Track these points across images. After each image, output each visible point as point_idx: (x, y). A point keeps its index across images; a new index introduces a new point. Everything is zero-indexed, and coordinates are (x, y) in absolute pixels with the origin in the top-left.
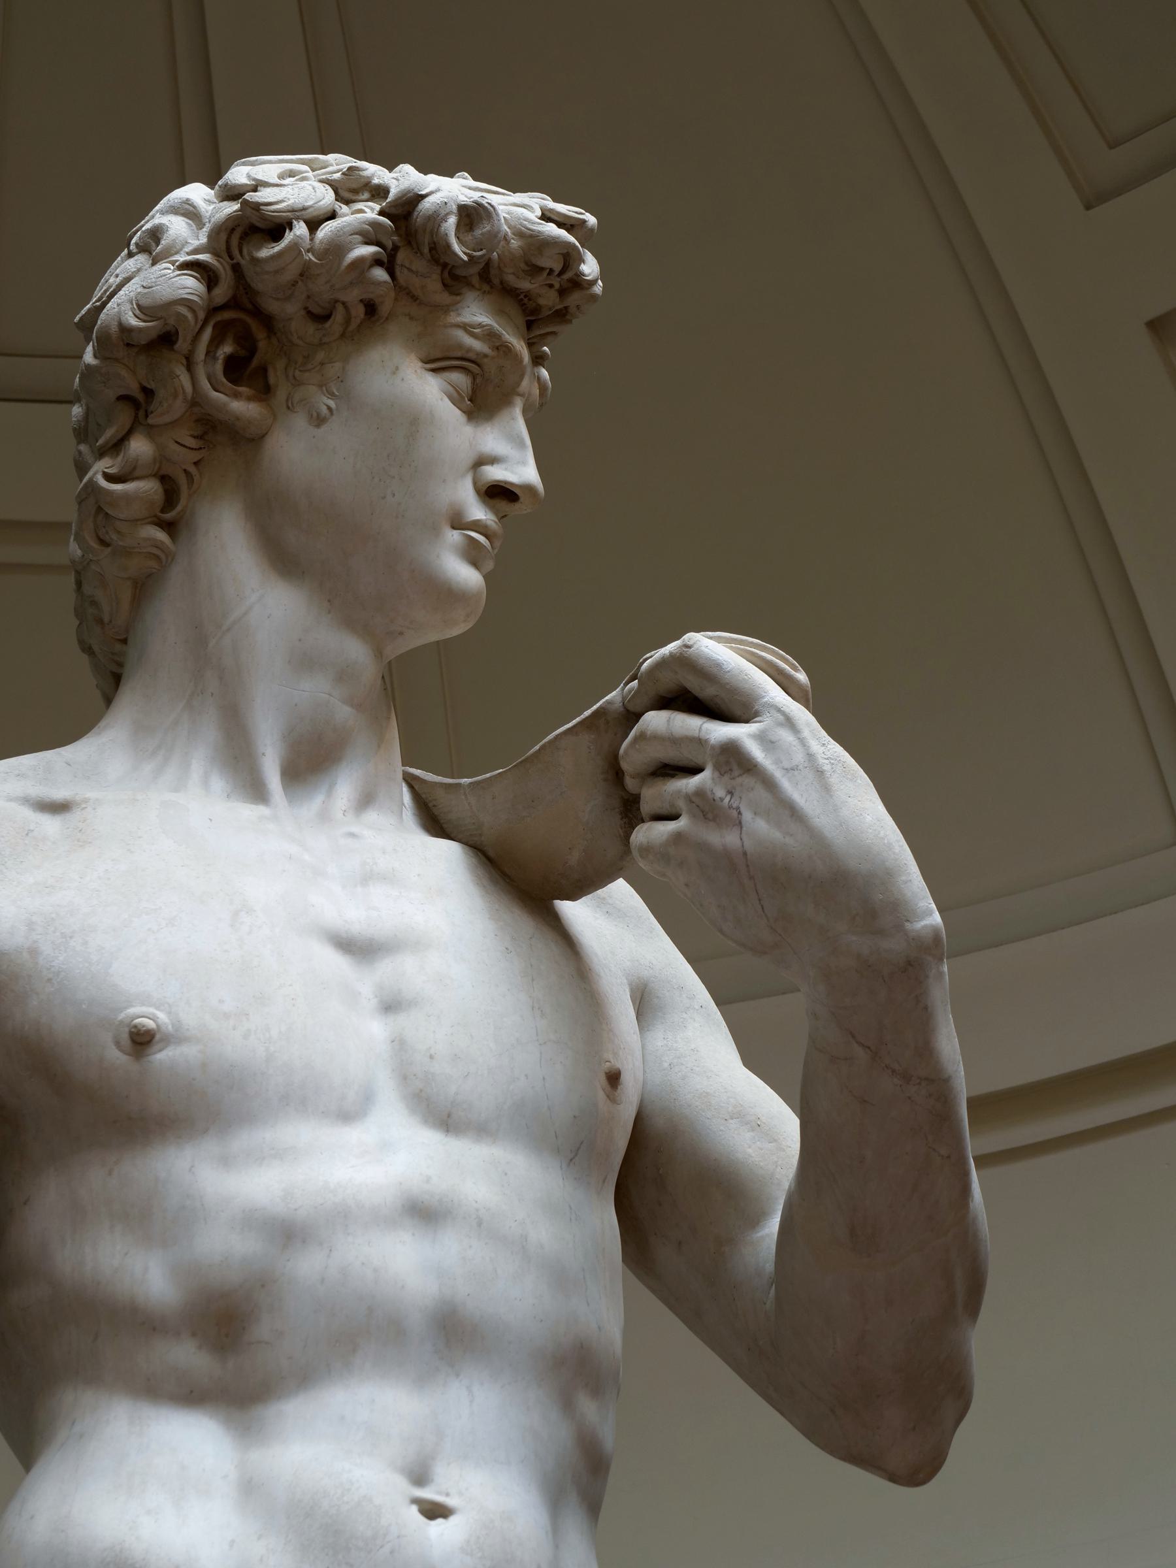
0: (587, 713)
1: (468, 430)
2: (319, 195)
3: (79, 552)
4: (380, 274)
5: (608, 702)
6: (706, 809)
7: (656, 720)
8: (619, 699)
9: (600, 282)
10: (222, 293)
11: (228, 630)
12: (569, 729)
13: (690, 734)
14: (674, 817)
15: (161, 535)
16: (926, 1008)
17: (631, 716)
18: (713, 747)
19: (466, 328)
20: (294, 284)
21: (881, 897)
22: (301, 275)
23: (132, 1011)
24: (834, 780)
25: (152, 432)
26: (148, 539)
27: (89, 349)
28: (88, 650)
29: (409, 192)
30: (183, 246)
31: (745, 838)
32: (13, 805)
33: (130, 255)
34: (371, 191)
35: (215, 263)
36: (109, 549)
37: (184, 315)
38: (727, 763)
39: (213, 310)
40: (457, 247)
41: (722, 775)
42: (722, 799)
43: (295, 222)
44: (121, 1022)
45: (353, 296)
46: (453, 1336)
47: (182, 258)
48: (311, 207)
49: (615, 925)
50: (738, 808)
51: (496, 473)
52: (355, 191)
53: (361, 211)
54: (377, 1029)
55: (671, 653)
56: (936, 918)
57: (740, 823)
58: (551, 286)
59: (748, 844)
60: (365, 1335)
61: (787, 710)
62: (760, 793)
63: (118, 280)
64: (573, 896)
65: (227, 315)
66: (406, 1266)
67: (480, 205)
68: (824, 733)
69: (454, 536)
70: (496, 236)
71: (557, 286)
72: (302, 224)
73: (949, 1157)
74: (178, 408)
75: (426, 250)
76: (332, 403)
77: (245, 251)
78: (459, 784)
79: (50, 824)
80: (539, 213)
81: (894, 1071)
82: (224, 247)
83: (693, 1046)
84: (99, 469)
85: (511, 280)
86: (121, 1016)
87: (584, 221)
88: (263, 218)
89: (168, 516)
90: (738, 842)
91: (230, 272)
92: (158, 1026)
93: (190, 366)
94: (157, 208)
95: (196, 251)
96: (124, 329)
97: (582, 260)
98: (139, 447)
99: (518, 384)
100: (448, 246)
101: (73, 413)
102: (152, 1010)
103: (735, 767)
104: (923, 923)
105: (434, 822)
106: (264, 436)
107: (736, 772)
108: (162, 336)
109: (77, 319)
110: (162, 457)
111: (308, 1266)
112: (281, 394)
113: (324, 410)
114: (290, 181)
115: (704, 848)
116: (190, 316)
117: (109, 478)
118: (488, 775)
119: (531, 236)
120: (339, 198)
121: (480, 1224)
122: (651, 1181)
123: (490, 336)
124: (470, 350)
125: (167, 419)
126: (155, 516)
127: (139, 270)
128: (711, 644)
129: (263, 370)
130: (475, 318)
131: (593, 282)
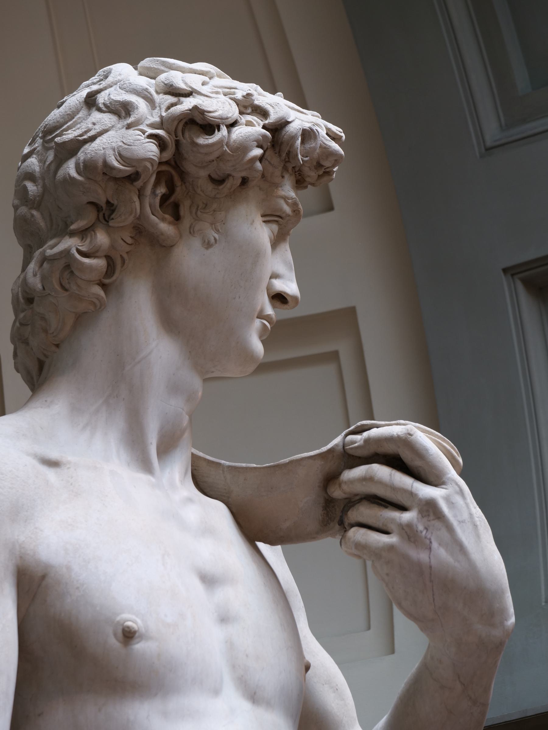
0: (324, 449)
3: (39, 286)
4: (258, 165)
5: (336, 445)
6: (409, 533)
7: (381, 471)
8: (341, 444)
11: (139, 362)
15: (102, 293)
18: (420, 500)
19: (285, 198)
21: (498, 605)
22: (218, 158)
23: (125, 616)
25: (109, 230)
26: (94, 294)
29: (283, 119)
34: (252, 108)
35: (168, 138)
36: (68, 293)
37: (148, 168)
38: (428, 511)
39: (160, 163)
40: (300, 157)
41: (423, 517)
43: (222, 126)
44: (118, 622)
47: (150, 131)
48: (230, 117)
50: (430, 539)
51: (280, 285)
52: (246, 107)
55: (399, 436)
57: (430, 548)
63: (98, 128)
65: (164, 168)
67: (312, 130)
69: (257, 323)
75: (284, 155)
76: (217, 236)
77: (187, 135)
78: (219, 464)
79: (51, 474)
84: (70, 243)
86: (118, 618)
89: (107, 281)
93: (140, 196)
95: (152, 126)
96: (106, 164)
98: (102, 238)
100: (297, 155)
102: (133, 617)
103: (431, 514)
106: (172, 246)
107: (432, 517)
110: (112, 246)
112: (187, 221)
113: (212, 240)
115: (406, 557)
116: (150, 167)
117: (78, 251)
119: (325, 148)
124: (284, 212)
125: (121, 225)
126: (100, 280)
127: (113, 126)
130: (290, 193)
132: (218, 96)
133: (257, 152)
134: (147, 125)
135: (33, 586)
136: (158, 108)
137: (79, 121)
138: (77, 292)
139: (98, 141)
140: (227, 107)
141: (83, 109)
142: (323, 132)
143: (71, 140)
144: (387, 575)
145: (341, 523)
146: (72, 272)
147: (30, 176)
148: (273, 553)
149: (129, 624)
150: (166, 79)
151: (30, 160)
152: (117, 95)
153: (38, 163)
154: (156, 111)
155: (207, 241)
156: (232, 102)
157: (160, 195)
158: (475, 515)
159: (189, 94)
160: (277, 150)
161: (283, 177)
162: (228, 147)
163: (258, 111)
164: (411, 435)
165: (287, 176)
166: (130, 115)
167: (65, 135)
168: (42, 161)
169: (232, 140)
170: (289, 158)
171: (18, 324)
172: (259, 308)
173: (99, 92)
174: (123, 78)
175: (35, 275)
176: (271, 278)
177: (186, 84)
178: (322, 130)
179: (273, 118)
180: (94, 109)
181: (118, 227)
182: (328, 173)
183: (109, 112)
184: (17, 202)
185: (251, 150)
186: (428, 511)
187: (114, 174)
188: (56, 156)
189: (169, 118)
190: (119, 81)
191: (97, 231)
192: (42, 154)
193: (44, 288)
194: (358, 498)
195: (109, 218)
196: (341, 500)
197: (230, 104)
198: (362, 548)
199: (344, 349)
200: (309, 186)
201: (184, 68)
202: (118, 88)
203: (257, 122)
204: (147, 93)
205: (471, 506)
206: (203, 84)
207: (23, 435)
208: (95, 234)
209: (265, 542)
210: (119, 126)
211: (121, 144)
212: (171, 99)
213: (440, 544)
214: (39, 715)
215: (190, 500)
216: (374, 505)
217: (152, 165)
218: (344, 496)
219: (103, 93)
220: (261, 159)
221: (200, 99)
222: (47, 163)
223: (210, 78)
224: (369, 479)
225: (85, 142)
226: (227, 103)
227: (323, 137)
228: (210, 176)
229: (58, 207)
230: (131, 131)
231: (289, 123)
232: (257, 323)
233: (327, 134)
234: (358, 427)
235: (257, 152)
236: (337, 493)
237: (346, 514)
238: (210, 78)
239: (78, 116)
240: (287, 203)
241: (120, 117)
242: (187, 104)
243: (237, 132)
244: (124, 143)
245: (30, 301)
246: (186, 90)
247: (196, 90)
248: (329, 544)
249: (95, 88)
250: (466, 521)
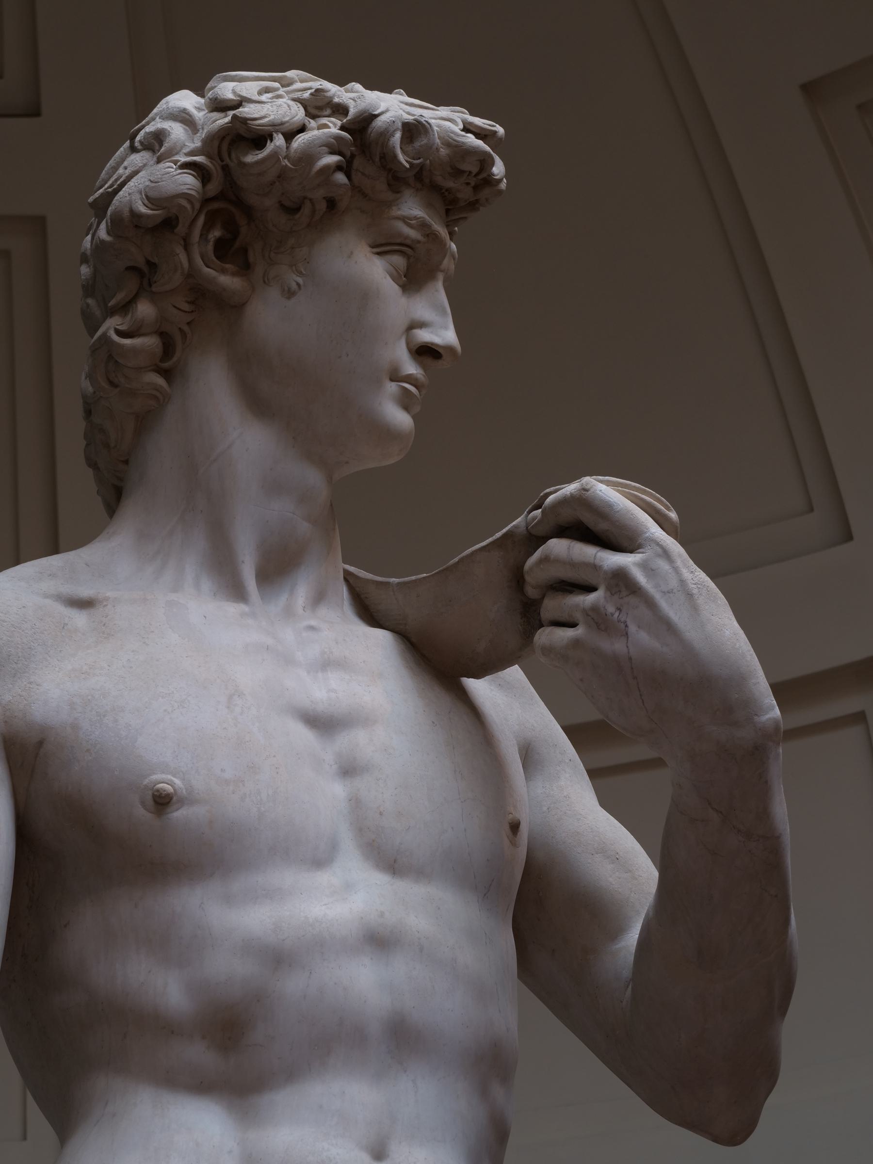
0: (498, 535)
1: (403, 301)
2: (293, 111)
3: (90, 389)
4: (341, 177)
5: (515, 527)
6: (598, 620)
7: (558, 546)
8: (523, 524)
9: (505, 180)
10: (213, 188)
14: (573, 625)
15: (160, 381)
16: (766, 782)
17: (534, 539)
18: (606, 572)
19: (405, 220)
20: (273, 183)
22: (279, 177)
23: (154, 777)
24: (700, 601)
27: (103, 226)
28: (92, 464)
30: (182, 148)
32: (48, 602)
33: (133, 149)
34: (332, 108)
35: (209, 164)
39: (206, 201)
40: (401, 157)
42: (612, 615)
43: (275, 135)
45: (319, 194)
46: (402, 1040)
47: (183, 159)
48: (287, 122)
49: (508, 699)
51: (425, 336)
52: (320, 108)
53: (326, 126)
54: (338, 790)
55: (571, 494)
56: (777, 712)
58: (468, 184)
60: (337, 1040)
61: (664, 544)
63: (128, 172)
64: (477, 676)
65: (216, 205)
66: (365, 984)
68: (691, 562)
69: (392, 388)
70: (431, 148)
71: (473, 184)
72: (281, 136)
73: (776, 896)
75: (377, 159)
76: (300, 280)
77: (233, 155)
78: (388, 583)
79: (79, 619)
80: (461, 126)
82: (216, 152)
83: (565, 794)
84: (110, 326)
85: (439, 180)
87: (495, 132)
88: (249, 130)
89: (166, 365)
92: (175, 790)
93: (187, 247)
94: (155, 111)
95: (192, 153)
96: (135, 215)
97: (493, 163)
98: (145, 309)
99: (441, 263)
100: (395, 156)
101: (82, 272)
102: (170, 777)
105: (369, 613)
108: (165, 221)
109: (91, 199)
111: (293, 985)
114: (270, 97)
116: (188, 206)
117: (119, 333)
118: (413, 578)
119: (456, 146)
120: (308, 114)
121: (421, 950)
122: (539, 906)
123: (423, 226)
124: (407, 237)
127: (145, 165)
128: (602, 487)
129: (245, 251)
130: (412, 212)
131: (501, 180)
133: (333, 159)
143: (102, 194)
144: (581, 680)
156: (291, 103)
162: (289, 161)
169: (292, 151)
185: (320, 158)
197: (289, 106)
204: (184, 115)
211: (148, 183)
212: (215, 115)
214: (65, 926)
226: (285, 106)
227: (453, 132)
228: (283, 207)
230: (161, 165)
235: (333, 159)
236: (531, 592)
247: (245, 98)
250: (675, 591)
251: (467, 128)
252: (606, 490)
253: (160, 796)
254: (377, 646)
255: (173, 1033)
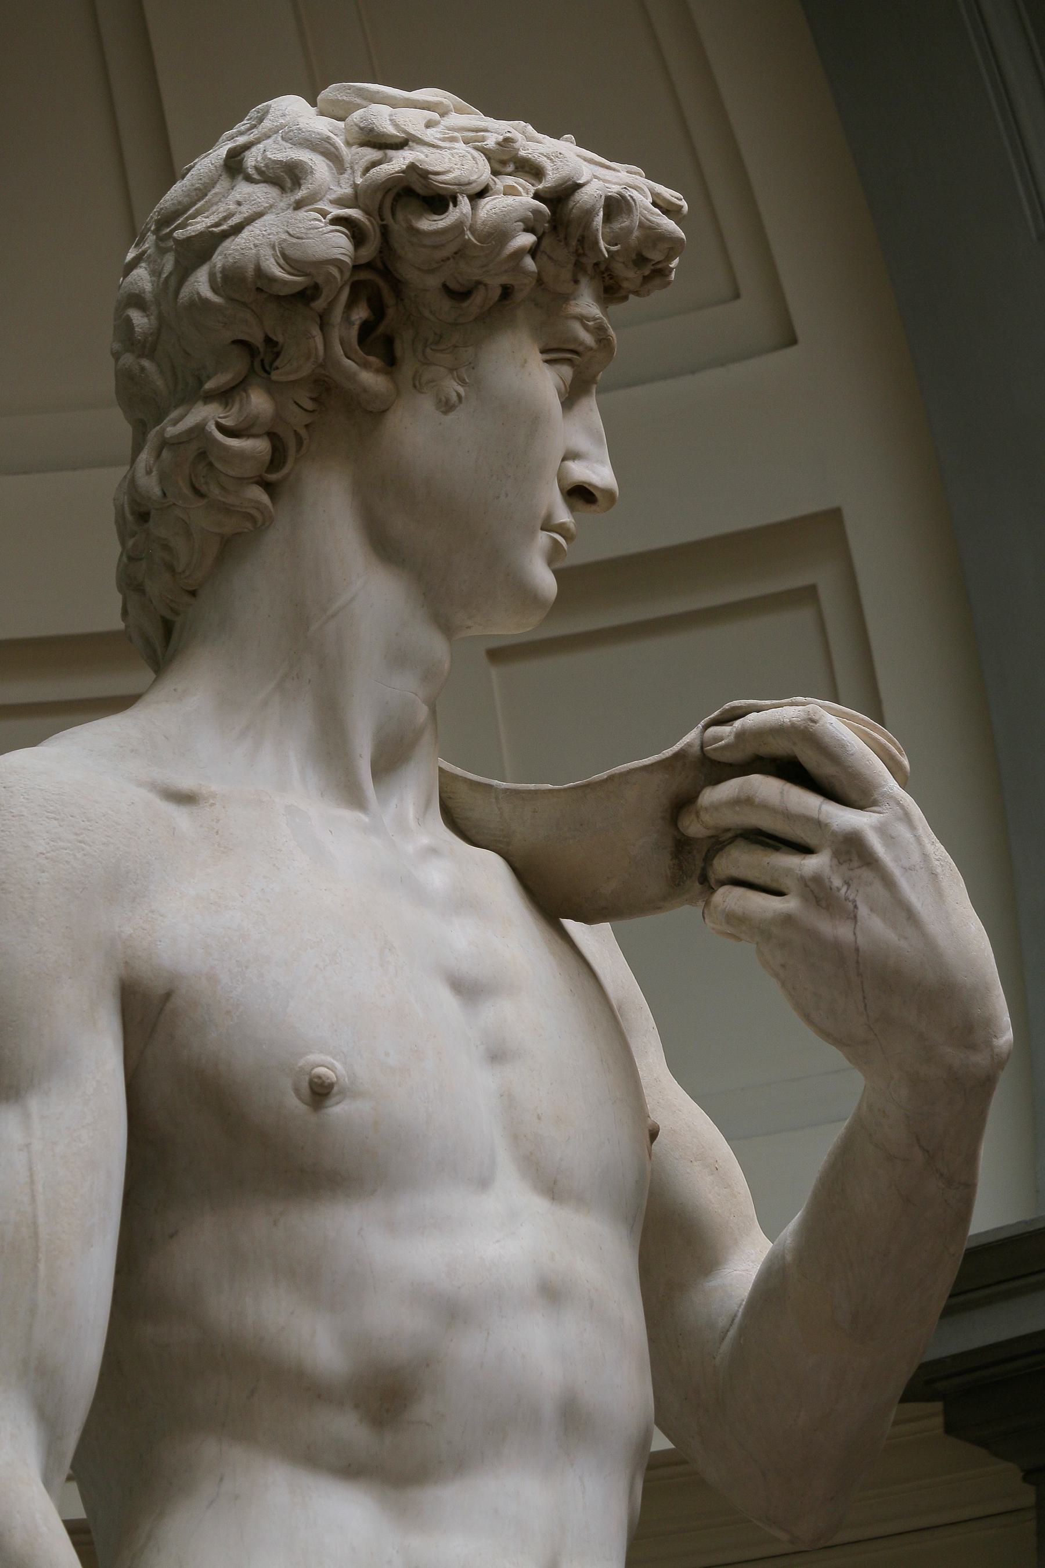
0: (668, 753)
3: (157, 491)
4: (529, 263)
5: (689, 745)
6: (817, 892)
7: (766, 787)
8: (698, 742)
10: (368, 253)
11: (333, 616)
12: (645, 768)
13: (808, 813)
14: (779, 893)
15: (265, 498)
17: (714, 767)
18: (834, 834)
19: (582, 319)
22: (456, 253)
25: (272, 389)
29: (569, 179)
31: (858, 932)
34: (515, 163)
36: (205, 501)
37: (335, 278)
38: (848, 852)
39: (356, 268)
40: (602, 244)
43: (460, 197)
47: (336, 211)
50: (854, 901)
51: (581, 472)
52: (504, 163)
57: (855, 917)
59: (861, 940)
61: (906, 805)
62: (878, 890)
63: (246, 211)
64: (587, 918)
65: (364, 275)
67: (623, 197)
69: (543, 539)
74: (307, 369)
75: (574, 243)
76: (461, 390)
77: (400, 216)
78: (491, 786)
79: (180, 817)
81: (942, 1175)
82: (377, 207)
84: (205, 414)
87: (682, 207)
89: (273, 477)
90: (850, 937)
91: (378, 234)
95: (340, 202)
96: (260, 272)
98: (258, 402)
100: (597, 243)
104: (1004, 1039)
106: (384, 411)
107: (856, 863)
110: (278, 417)
111: (468, 1349)
112: (407, 369)
113: (454, 398)
115: (813, 934)
119: (650, 228)
124: (582, 343)
125: (292, 378)
127: (271, 206)
128: (834, 719)
129: (389, 342)
130: (591, 310)
132: (456, 145)
133: (526, 239)
134: (331, 202)
135: (148, 1013)
136: (349, 171)
137: (216, 199)
138: (220, 498)
139: (245, 233)
140: (469, 164)
141: (222, 178)
142: (644, 201)
143: (201, 234)
144: (783, 966)
145: (704, 879)
146: (210, 464)
147: (137, 301)
148: (595, 939)
149: (321, 1070)
150: (363, 119)
151: (135, 272)
152: (276, 151)
153: (148, 277)
154: (346, 176)
155: (443, 399)
156: (476, 153)
157: (358, 323)
158: (933, 856)
159: (401, 144)
160: (562, 236)
161: (576, 282)
162: (473, 233)
163: (527, 169)
164: (814, 722)
165: (584, 281)
166: (300, 185)
167: (191, 224)
168: (155, 273)
169: (479, 222)
170: (583, 248)
171: (125, 559)
172: (543, 513)
173: (247, 147)
174: (292, 119)
175: (149, 472)
176: (564, 459)
177: (396, 126)
178: (646, 197)
179: (551, 179)
180: (240, 177)
181: (287, 383)
182: (660, 273)
183: (265, 182)
184: (117, 346)
185: (514, 237)
186: (848, 852)
187: (276, 289)
188: (177, 263)
189: (368, 186)
190: (282, 126)
191: (250, 391)
192: (155, 261)
193: (165, 494)
194: (730, 835)
195: (271, 365)
196: (702, 839)
197: (474, 158)
198: (737, 921)
199: (824, 578)
200: (631, 296)
201: (394, 98)
202: (279, 139)
203: (524, 188)
205: (926, 841)
206: (429, 125)
207: (132, 751)
208: (248, 396)
209: (576, 919)
210: (282, 204)
211: (284, 236)
213: (871, 910)
214: (171, 1236)
215: (433, 851)
216: (753, 847)
217: (341, 271)
218: (709, 833)
219: (254, 149)
220: (533, 251)
221: (422, 152)
222: (164, 276)
223: (442, 115)
224: (746, 801)
225: (225, 235)
227: (646, 208)
228: (445, 286)
229: (185, 351)
230: (302, 214)
231: (580, 186)
232: (543, 539)
233: (654, 204)
234: (727, 711)
235: (526, 239)
236: (693, 827)
237: (711, 865)
238: (442, 115)
239: (213, 191)
240: (586, 328)
241: (283, 189)
242: (399, 161)
243: (488, 207)
244: (290, 235)
245: (143, 517)
246: (397, 136)
248: (683, 915)
249: (241, 140)
250: (917, 867)
251: (658, 203)
252: (841, 726)
253: (322, 1085)
254: (489, 873)
255: (319, 1396)
